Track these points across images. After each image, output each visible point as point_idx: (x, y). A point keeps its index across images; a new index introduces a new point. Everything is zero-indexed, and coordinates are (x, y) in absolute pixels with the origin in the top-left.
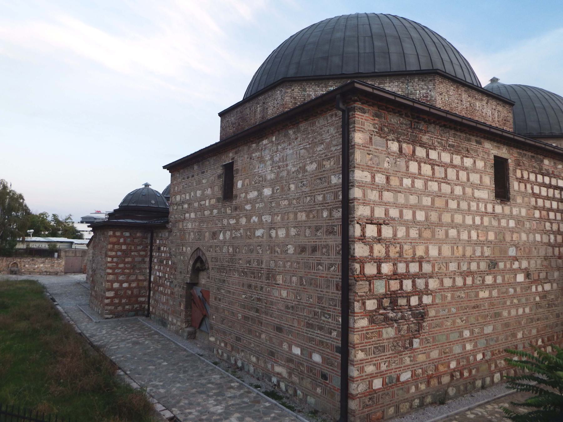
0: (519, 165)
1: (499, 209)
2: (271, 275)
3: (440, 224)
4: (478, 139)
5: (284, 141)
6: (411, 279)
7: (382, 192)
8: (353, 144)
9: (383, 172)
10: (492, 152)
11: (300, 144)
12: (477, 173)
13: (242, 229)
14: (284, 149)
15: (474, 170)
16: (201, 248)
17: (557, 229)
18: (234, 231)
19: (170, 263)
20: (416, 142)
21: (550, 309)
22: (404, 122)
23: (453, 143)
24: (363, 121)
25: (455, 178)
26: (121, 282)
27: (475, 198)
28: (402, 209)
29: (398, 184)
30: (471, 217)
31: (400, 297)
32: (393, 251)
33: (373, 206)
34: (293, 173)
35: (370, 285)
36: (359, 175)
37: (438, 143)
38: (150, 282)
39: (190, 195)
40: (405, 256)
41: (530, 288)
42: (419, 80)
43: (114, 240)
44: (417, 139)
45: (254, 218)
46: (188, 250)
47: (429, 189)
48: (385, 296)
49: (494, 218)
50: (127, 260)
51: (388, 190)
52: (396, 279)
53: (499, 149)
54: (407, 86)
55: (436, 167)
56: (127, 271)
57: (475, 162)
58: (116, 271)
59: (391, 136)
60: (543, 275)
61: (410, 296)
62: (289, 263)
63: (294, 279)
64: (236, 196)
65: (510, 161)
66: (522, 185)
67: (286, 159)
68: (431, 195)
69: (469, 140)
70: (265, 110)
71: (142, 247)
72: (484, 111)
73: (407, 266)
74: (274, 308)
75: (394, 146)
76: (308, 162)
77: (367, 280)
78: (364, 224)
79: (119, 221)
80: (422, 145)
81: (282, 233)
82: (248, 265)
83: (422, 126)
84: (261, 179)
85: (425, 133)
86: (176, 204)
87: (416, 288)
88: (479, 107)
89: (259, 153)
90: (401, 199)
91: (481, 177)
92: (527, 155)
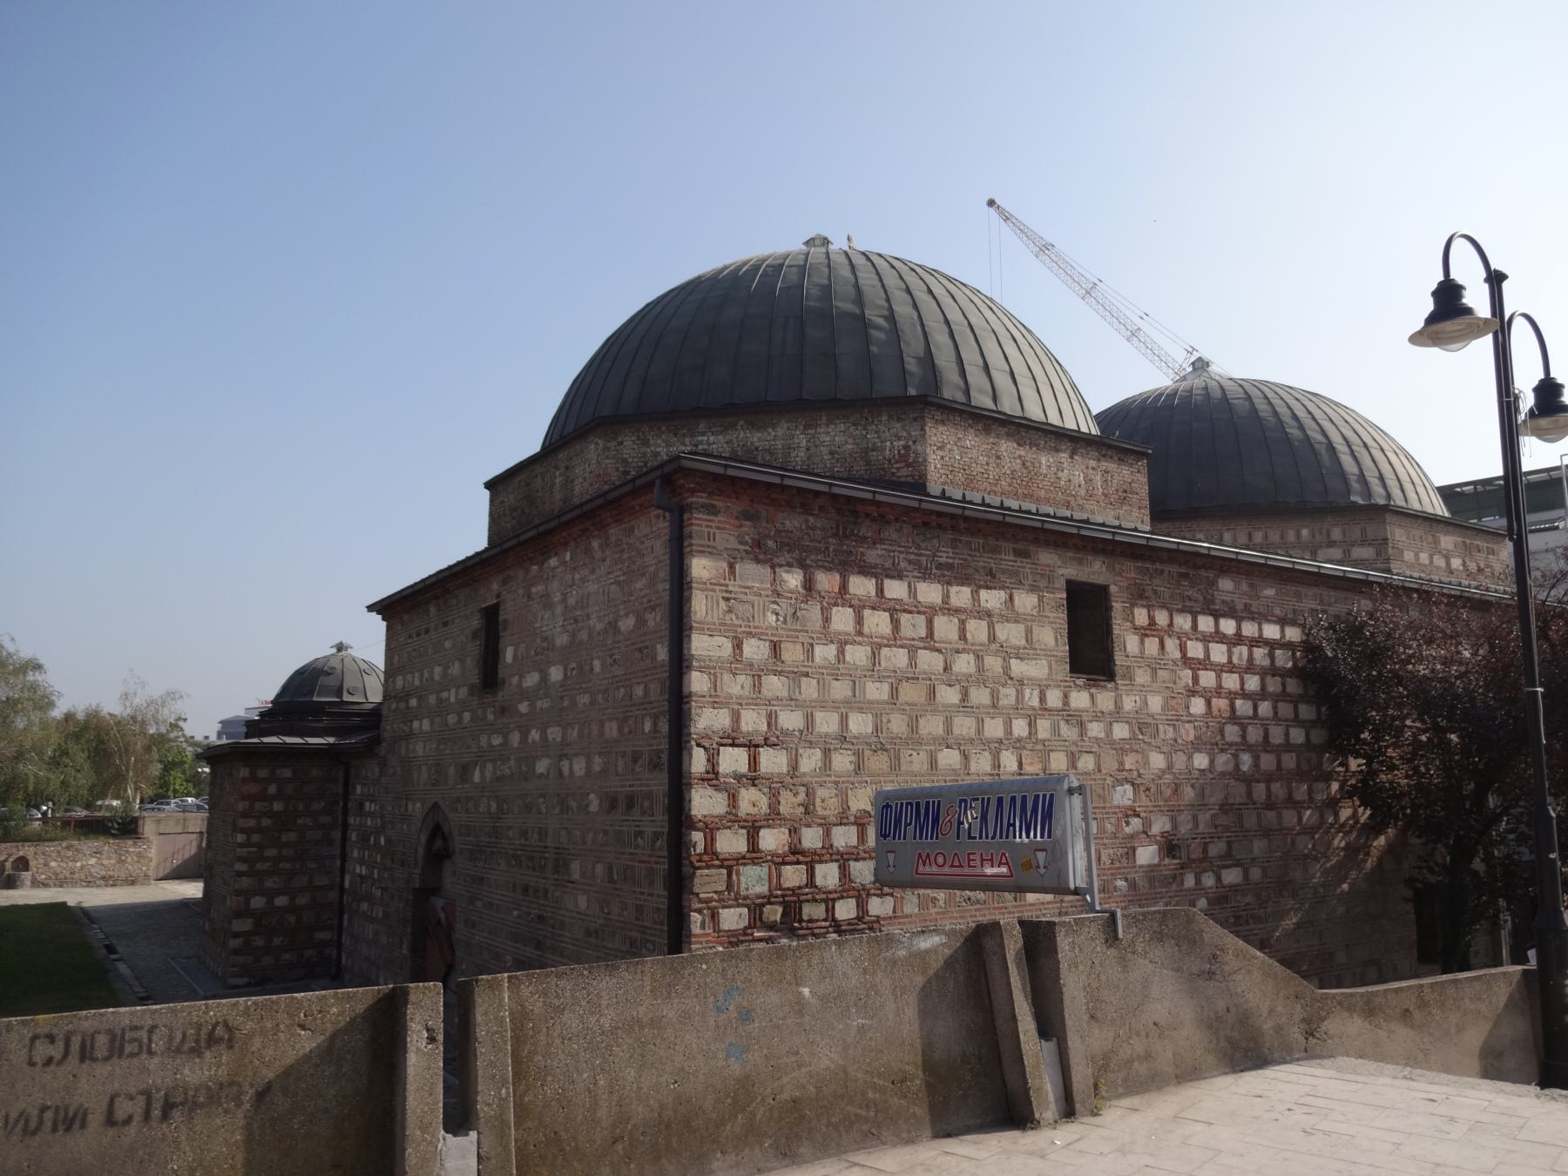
0: (1141, 597)
1: (1080, 699)
2: (561, 864)
4: (1020, 546)
5: (584, 565)
6: (837, 861)
7: (759, 676)
8: (689, 579)
9: (762, 634)
10: (1061, 571)
11: (609, 573)
12: (1017, 621)
13: (512, 757)
14: (584, 580)
15: (1010, 614)
16: (441, 803)
17: (1261, 739)
18: (499, 763)
19: (382, 841)
20: (847, 565)
21: (1240, 928)
22: (819, 525)
23: (951, 561)
24: (711, 531)
25: (956, 637)
26: (270, 895)
27: (1011, 679)
28: (813, 710)
31: (808, 901)
32: (789, 803)
33: (736, 707)
34: (599, 634)
35: (729, 875)
36: (701, 645)
37: (910, 562)
38: (342, 890)
39: (422, 676)
41: (1177, 878)
42: (890, 417)
43: (253, 788)
44: (853, 558)
45: (533, 732)
46: (417, 808)
47: (883, 664)
48: (769, 899)
49: (1067, 721)
50: (285, 838)
51: (777, 673)
52: (798, 863)
54: (864, 432)
56: (287, 865)
57: (1011, 598)
58: (259, 866)
59: (786, 557)
60: (1216, 849)
61: (834, 900)
62: (591, 835)
63: (599, 868)
64: (504, 682)
65: (1113, 589)
66: (1152, 645)
67: (587, 603)
68: (889, 677)
69: (995, 550)
70: (568, 482)
71: (323, 804)
72: (1064, 475)
73: (827, 834)
74: (564, 936)
75: (793, 580)
76: (622, 613)
77: (722, 867)
78: (715, 746)
79: (266, 740)
80: (865, 570)
81: (579, 767)
82: (523, 841)
83: (865, 530)
84: (545, 645)
85: (874, 544)
86: (395, 697)
87: (851, 881)
88: (1049, 467)
89: (543, 587)
92: (1166, 574)
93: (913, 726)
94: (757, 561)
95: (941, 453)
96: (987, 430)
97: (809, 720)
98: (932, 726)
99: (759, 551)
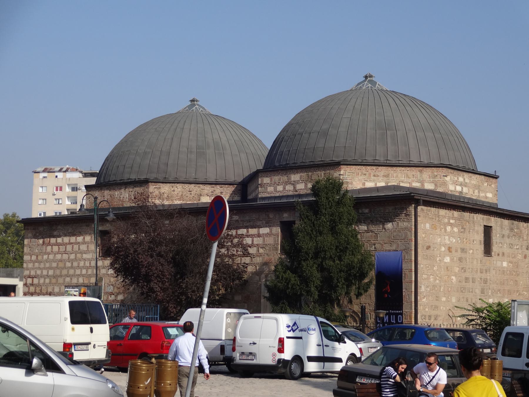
3: (61, 276)
15: (84, 242)
29: (41, 258)
30: (80, 270)
37: (62, 233)
40: (43, 292)
51: (36, 262)
53: (103, 225)
55: (61, 247)
57: (84, 238)
75: (41, 241)
80: (54, 237)
90: (42, 265)
91: (88, 246)
93: (61, 272)
94: (35, 238)
95: (89, 199)
96: (101, 189)
97: (42, 272)
98: (65, 272)
99: (36, 237)
